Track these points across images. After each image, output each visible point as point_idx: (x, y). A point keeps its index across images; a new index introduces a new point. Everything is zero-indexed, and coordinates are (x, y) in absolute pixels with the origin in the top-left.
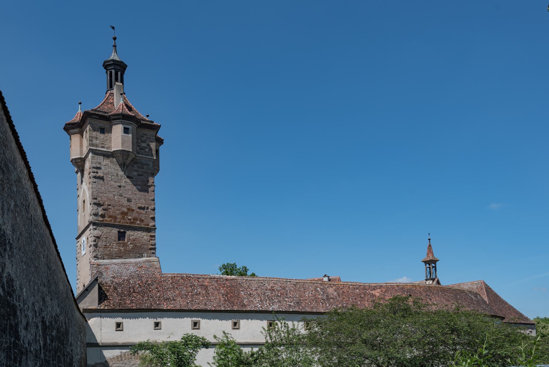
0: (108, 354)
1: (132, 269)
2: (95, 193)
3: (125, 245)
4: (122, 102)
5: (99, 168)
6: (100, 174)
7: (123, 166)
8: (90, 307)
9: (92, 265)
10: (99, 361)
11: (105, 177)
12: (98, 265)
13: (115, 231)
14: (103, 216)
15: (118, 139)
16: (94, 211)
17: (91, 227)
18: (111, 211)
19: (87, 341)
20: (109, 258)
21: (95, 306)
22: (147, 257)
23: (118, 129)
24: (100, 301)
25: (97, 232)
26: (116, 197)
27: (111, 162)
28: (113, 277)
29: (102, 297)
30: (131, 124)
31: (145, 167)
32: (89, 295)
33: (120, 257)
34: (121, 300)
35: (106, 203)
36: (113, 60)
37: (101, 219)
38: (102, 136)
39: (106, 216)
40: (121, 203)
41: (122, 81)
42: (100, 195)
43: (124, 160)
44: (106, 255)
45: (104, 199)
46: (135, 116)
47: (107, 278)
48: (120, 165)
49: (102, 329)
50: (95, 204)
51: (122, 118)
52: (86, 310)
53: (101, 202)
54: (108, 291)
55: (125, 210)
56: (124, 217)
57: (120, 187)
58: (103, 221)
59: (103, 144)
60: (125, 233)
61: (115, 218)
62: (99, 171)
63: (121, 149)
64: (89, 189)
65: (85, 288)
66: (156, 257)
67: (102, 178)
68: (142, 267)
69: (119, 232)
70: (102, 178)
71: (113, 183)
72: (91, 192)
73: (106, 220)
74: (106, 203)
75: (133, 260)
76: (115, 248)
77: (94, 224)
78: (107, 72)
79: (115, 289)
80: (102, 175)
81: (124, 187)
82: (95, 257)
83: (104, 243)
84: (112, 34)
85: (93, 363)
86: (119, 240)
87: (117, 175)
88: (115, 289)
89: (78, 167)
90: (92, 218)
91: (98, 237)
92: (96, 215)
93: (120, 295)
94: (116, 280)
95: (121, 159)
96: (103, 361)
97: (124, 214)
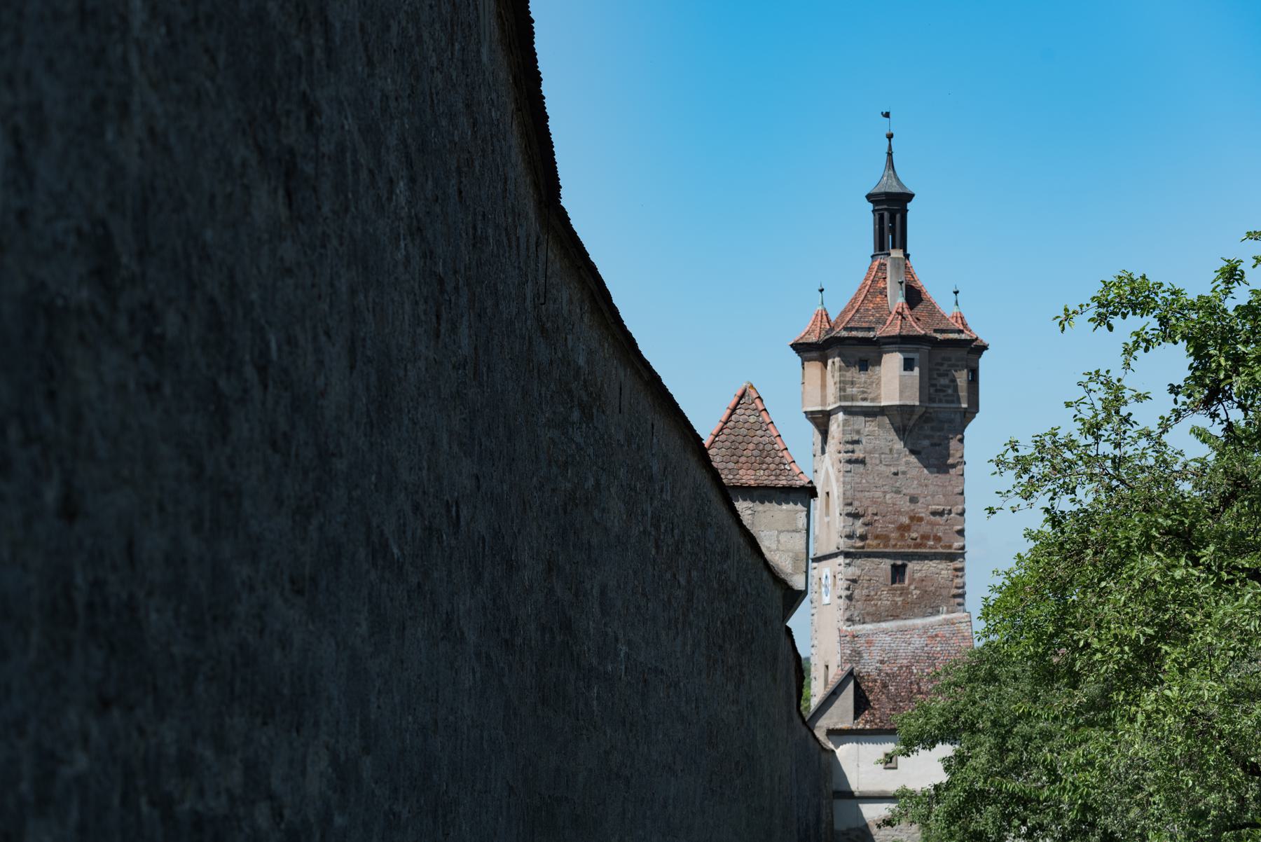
0: (872, 813)
1: (918, 642)
2: (849, 494)
3: (905, 592)
4: (901, 300)
5: (857, 442)
6: (859, 454)
7: (902, 431)
8: (840, 726)
9: (842, 636)
10: (853, 825)
11: (867, 460)
12: (854, 636)
13: (886, 565)
14: (863, 538)
15: (893, 381)
16: (848, 530)
17: (841, 559)
18: (879, 528)
19: (834, 788)
20: (873, 621)
21: (847, 723)
22: (948, 612)
23: (892, 362)
24: (858, 711)
25: (853, 571)
26: (888, 496)
27: (879, 426)
28: (882, 662)
29: (861, 704)
30: (917, 350)
31: (946, 426)
32: (837, 703)
33: (895, 617)
34: (894, 709)
35: (870, 511)
36: (887, 194)
37: (861, 544)
38: (862, 377)
39: (869, 536)
40: (897, 508)
41: (904, 247)
42: (858, 495)
43: (905, 422)
44: (868, 614)
45: (867, 503)
46: (925, 335)
47: (869, 666)
48: (897, 430)
49: (861, 765)
50: (848, 515)
51: (901, 342)
52: (831, 733)
53: (861, 511)
54: (871, 691)
55: (905, 520)
56: (902, 536)
57: (896, 474)
58: (863, 547)
59: (864, 392)
60: (904, 566)
61: (884, 538)
62: (856, 447)
63: (897, 403)
64: (837, 481)
65: (830, 687)
66: (964, 611)
67: (862, 462)
68: (937, 636)
69: (894, 566)
70: (862, 462)
71: (882, 468)
72: (841, 490)
73: (869, 546)
74: (870, 511)
75: (919, 622)
76: (886, 599)
77: (847, 555)
78: (874, 211)
79: (885, 686)
80: (861, 456)
81: (904, 473)
82: (848, 620)
83: (865, 592)
84: (884, 126)
85: (844, 828)
86: (893, 582)
87: (891, 450)
88: (885, 686)
89: (817, 425)
90: (844, 544)
91: (854, 581)
92: (849, 537)
93: (892, 698)
94: (886, 668)
95: (898, 420)
96: (861, 824)
97: (903, 529)
